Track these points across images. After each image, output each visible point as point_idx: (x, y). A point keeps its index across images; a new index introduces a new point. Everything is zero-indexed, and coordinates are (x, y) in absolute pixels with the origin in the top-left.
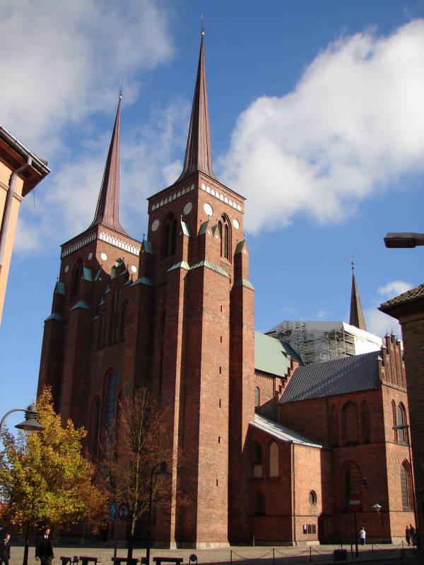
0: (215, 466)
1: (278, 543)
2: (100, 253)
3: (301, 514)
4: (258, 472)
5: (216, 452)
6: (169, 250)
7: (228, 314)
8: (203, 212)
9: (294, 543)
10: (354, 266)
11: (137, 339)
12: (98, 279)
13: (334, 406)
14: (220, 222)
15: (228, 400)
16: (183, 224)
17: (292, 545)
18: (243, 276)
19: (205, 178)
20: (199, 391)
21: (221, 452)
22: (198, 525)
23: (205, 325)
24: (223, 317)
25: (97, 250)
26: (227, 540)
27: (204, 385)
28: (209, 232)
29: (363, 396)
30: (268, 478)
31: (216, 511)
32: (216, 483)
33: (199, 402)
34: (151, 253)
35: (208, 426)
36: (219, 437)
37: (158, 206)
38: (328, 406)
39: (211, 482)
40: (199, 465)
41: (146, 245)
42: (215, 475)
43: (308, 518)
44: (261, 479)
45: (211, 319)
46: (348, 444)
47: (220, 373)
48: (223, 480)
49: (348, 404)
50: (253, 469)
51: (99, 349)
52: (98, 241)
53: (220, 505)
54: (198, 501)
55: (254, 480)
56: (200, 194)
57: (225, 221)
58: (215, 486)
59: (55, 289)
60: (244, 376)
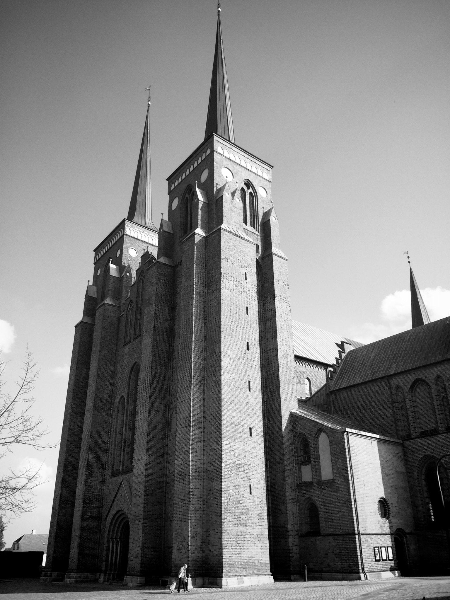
0: (246, 466)
1: (340, 575)
2: (128, 248)
3: (368, 531)
4: (307, 473)
5: (248, 448)
6: (189, 224)
7: (255, 283)
8: (221, 175)
9: (362, 575)
10: (410, 260)
11: (155, 323)
12: (126, 274)
13: (398, 387)
14: (242, 189)
15: (259, 381)
16: (198, 190)
17: (359, 578)
18: (273, 245)
19: (221, 141)
20: (220, 370)
21: (255, 448)
22: (224, 551)
23: (224, 293)
24: (248, 286)
25: (124, 246)
26: (269, 572)
27: (225, 363)
28: (227, 196)
29: (435, 371)
30: (320, 483)
31: (250, 530)
32: (249, 491)
33: (220, 385)
34: (172, 232)
35: (234, 414)
36: (250, 429)
37: (176, 184)
38: (390, 388)
39: (242, 489)
40: (223, 465)
41: (164, 225)
42: (246, 479)
43: (379, 536)
44: (311, 483)
45: (232, 287)
46: (424, 434)
47: (248, 349)
48: (259, 486)
49: (417, 381)
50: (300, 469)
51: (125, 345)
52: (125, 236)
53: (256, 520)
54: (223, 516)
55: (302, 486)
56: (216, 157)
57: (248, 188)
58: (247, 495)
59: (87, 293)
60: (280, 354)
